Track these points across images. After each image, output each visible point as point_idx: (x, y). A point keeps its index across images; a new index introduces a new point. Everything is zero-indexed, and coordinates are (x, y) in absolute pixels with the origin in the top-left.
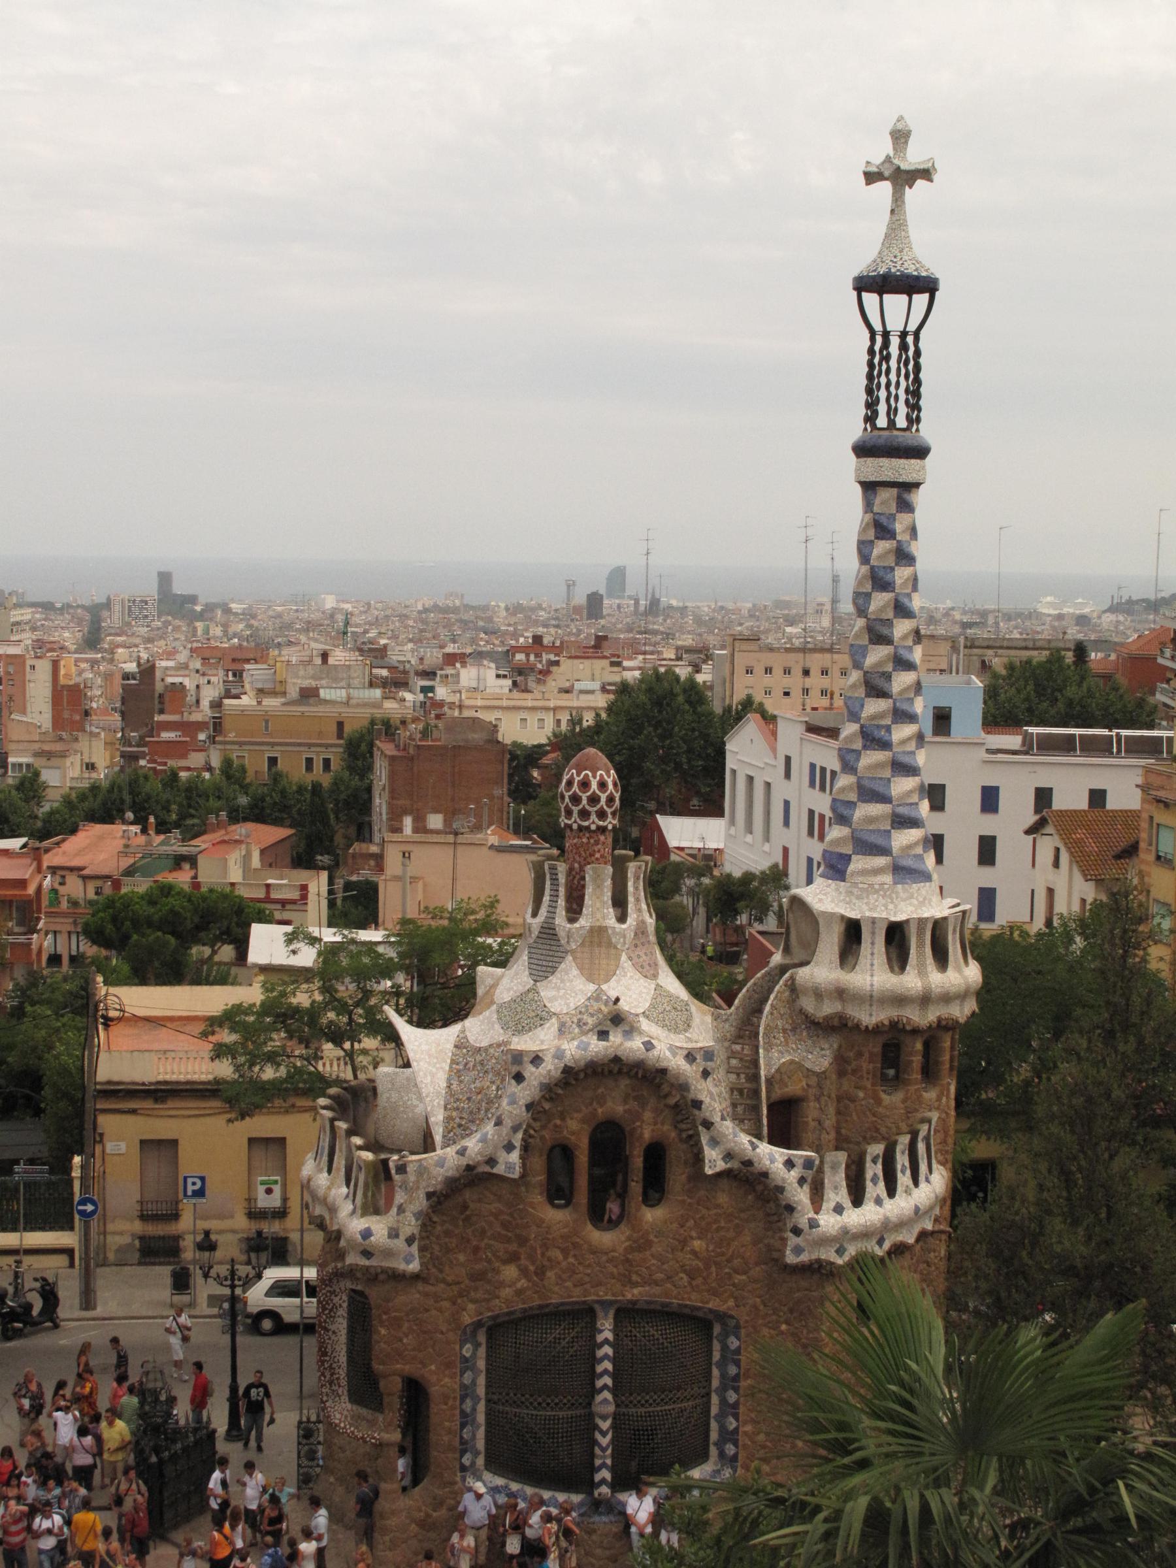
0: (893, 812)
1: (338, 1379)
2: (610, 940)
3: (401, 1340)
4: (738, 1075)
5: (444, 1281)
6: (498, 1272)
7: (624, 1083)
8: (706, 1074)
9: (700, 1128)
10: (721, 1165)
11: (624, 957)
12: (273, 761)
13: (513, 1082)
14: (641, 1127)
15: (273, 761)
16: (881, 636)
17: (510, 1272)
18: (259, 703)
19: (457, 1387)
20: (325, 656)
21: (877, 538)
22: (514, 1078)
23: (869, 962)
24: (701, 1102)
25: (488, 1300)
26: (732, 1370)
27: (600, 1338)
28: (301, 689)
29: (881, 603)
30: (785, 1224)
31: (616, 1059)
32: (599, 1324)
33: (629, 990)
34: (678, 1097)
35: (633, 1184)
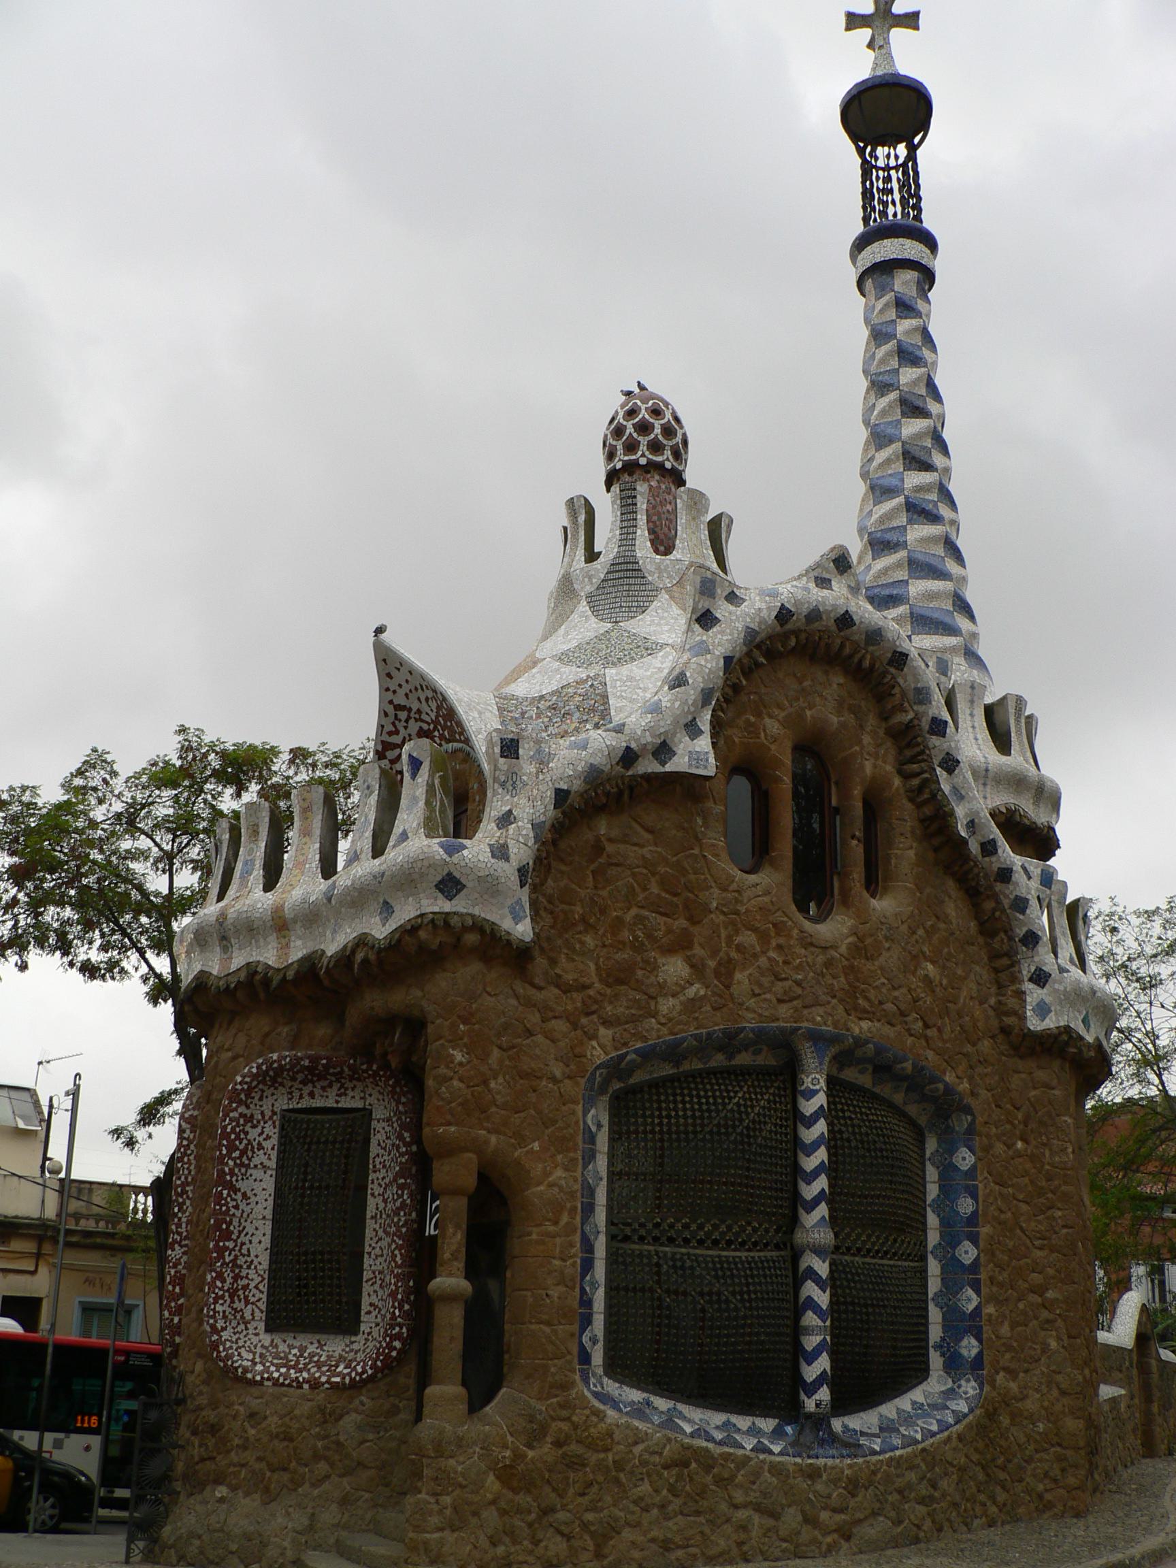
1: (245, 1287)
3: (485, 1082)
5: (558, 982)
6: (654, 968)
7: (838, 679)
9: (938, 770)
13: (697, 627)
16: (917, 408)
17: (674, 968)
19: (577, 1187)
21: (901, 317)
22: (698, 620)
23: (971, 737)
25: (634, 1020)
26: (966, 1206)
27: (809, 1107)
29: (914, 376)
30: (1020, 972)
31: (846, 620)
32: (808, 1082)
34: (911, 715)
35: (855, 842)
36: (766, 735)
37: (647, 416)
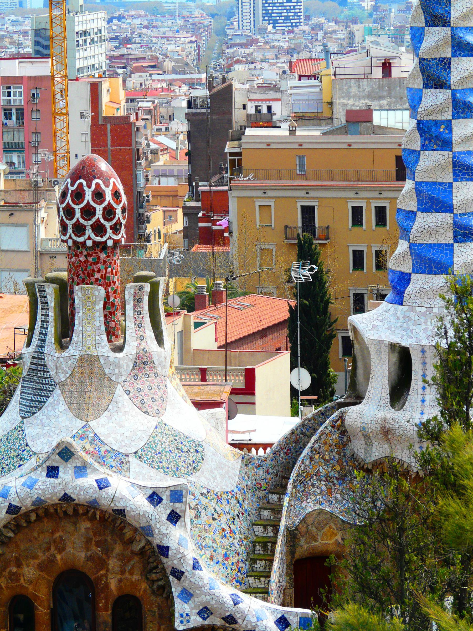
0: (455, 224)
2: (101, 368)
4: (265, 527)
7: (85, 525)
8: (174, 517)
9: (171, 578)
10: (196, 621)
11: (119, 390)
12: (308, 213)
14: (106, 576)
15: (308, 213)
18: (292, 132)
20: (387, 67)
23: (420, 397)
24: (168, 548)
28: (349, 113)
31: (66, 498)
33: (121, 426)
34: (143, 544)
36: (24, 580)
37: (71, 203)
